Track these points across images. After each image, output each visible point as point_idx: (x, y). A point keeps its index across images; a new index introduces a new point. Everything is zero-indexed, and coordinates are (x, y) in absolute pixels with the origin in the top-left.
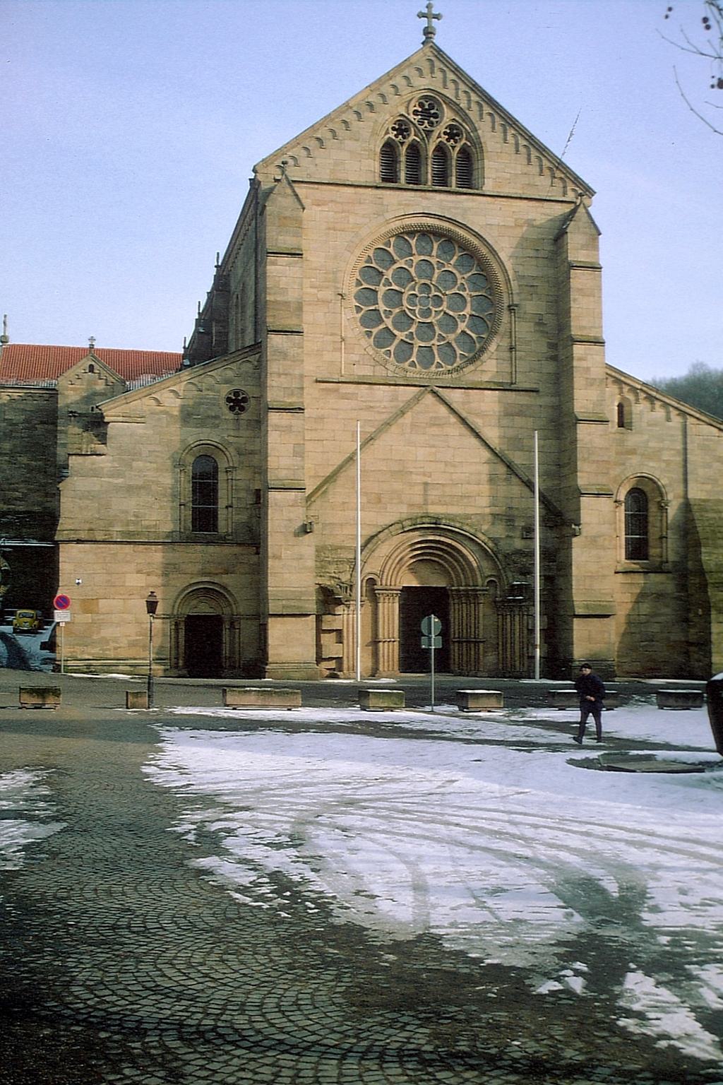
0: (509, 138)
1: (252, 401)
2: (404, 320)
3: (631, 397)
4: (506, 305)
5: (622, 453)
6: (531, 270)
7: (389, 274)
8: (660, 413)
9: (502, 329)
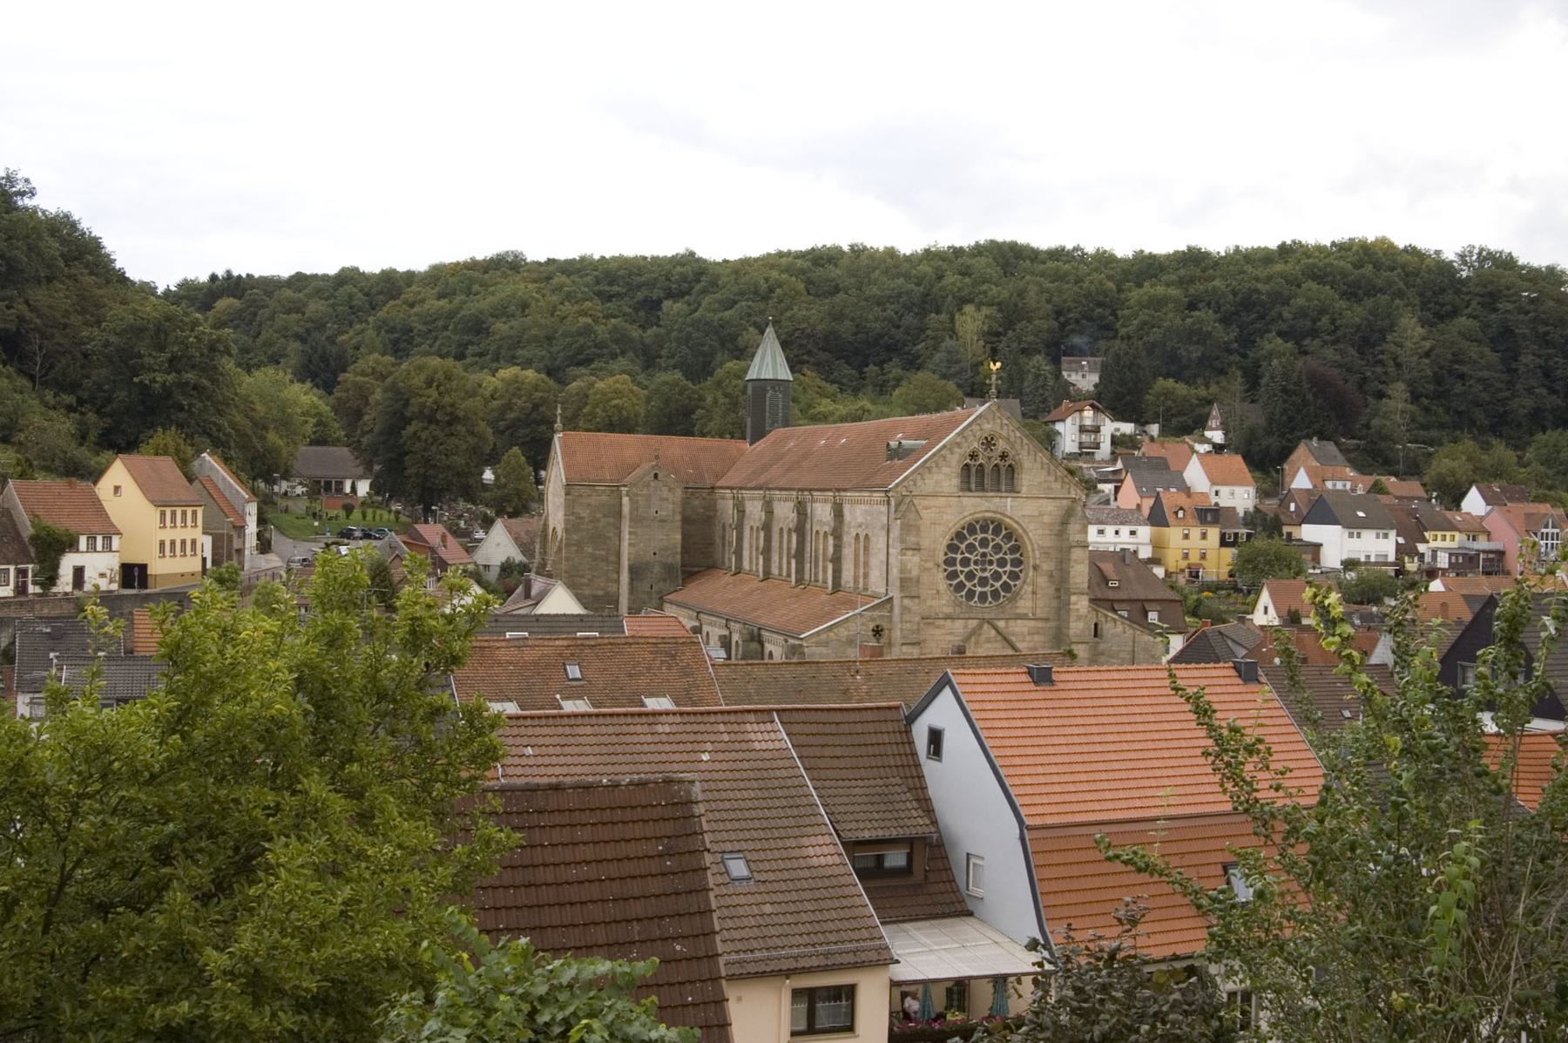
0: (1038, 459)
1: (886, 632)
2: (970, 576)
3: (1103, 619)
8: (1120, 628)
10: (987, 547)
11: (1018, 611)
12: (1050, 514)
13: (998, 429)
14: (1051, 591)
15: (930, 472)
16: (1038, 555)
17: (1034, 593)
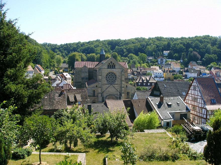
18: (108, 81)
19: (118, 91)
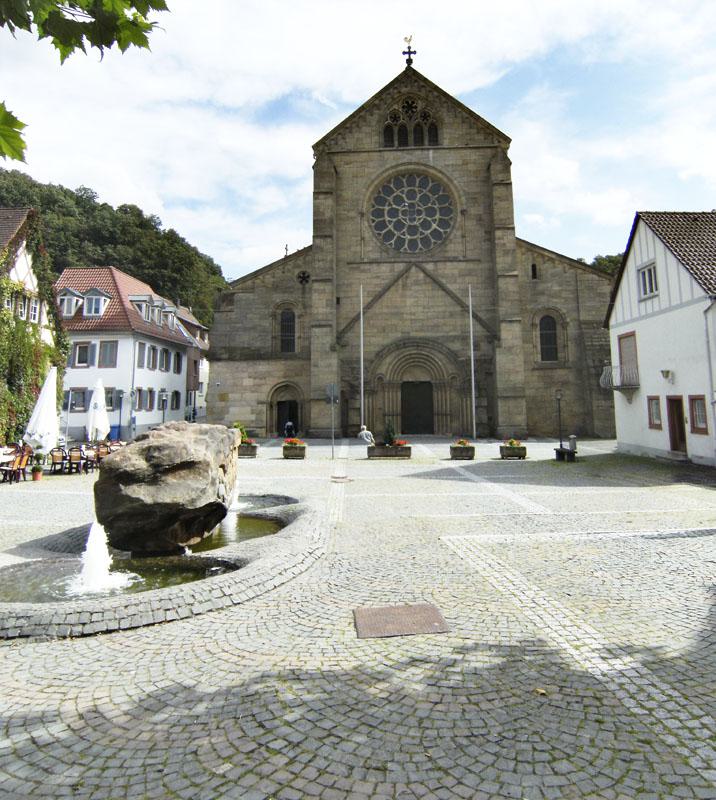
2: (399, 225)
4: (459, 211)
5: (534, 294)
6: (474, 189)
7: (390, 199)
9: (457, 225)
10: (414, 199)
11: (449, 254)
12: (474, 163)
13: (415, 89)
14: (481, 233)
15: (351, 132)
16: (463, 198)
17: (463, 236)
18: (389, 235)
19: (464, 308)
